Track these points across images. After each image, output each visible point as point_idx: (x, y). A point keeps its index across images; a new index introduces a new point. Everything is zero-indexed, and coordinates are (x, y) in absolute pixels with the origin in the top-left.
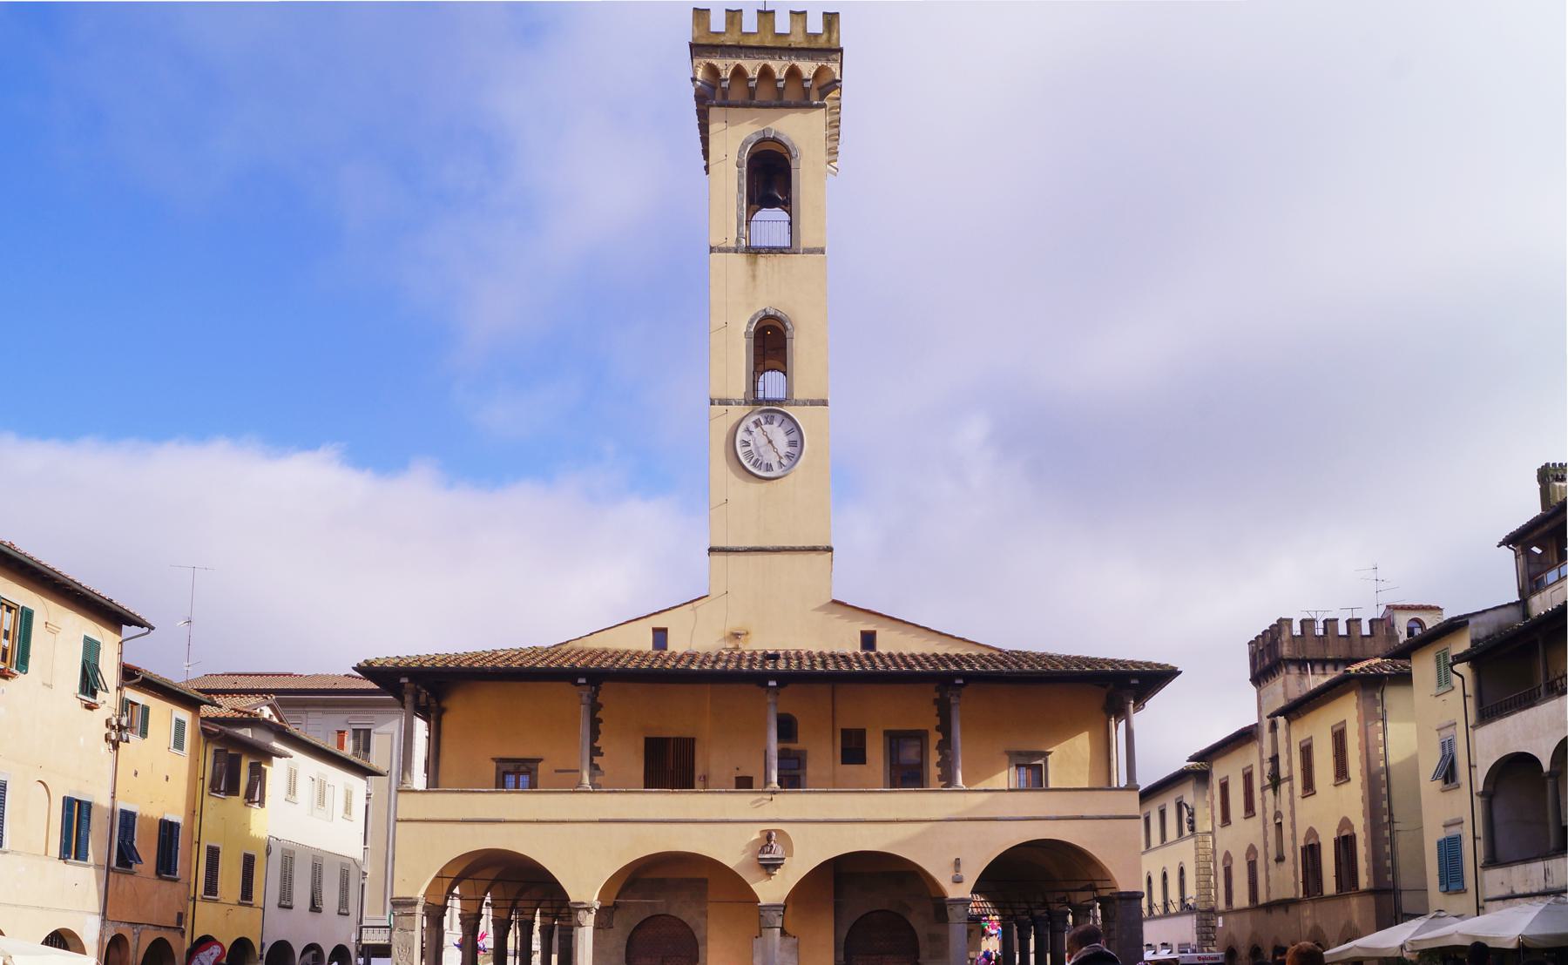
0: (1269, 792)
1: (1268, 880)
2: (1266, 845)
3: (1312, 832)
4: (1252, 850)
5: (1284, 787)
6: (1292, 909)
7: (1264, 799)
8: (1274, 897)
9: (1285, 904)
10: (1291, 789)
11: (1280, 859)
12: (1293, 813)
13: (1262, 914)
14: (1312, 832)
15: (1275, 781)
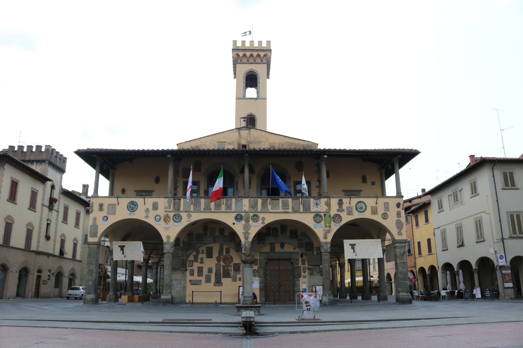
0: (46, 210)
1: (39, 242)
2: (40, 228)
3: (63, 235)
4: (75, 239)
5: (54, 213)
6: (51, 258)
7: (42, 210)
8: (40, 249)
9: (48, 255)
10: (58, 216)
11: (48, 238)
12: (57, 224)
13: (34, 255)
14: (63, 235)
15: (51, 208)
